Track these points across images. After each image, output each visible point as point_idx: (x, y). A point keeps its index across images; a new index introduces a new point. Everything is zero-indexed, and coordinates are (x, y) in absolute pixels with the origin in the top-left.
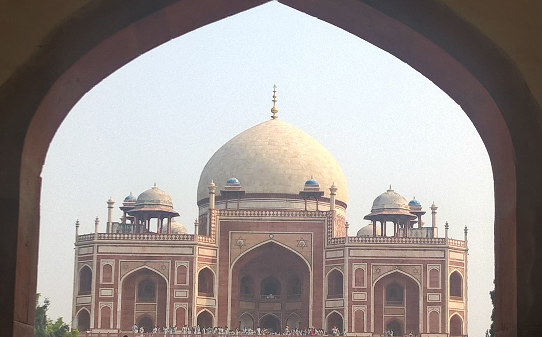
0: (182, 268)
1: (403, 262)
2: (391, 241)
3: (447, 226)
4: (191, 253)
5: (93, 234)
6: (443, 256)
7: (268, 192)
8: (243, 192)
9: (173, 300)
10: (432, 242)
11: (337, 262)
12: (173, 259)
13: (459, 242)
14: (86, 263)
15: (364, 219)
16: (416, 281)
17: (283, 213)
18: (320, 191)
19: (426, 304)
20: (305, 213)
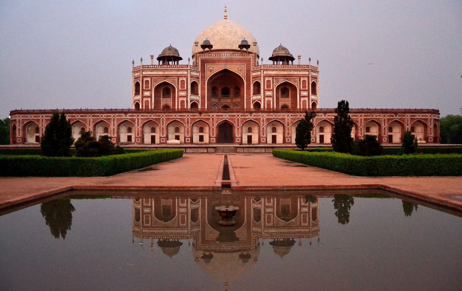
0: (183, 81)
1: (289, 76)
2: (283, 67)
3: (310, 59)
4: (187, 74)
5: (140, 66)
6: (308, 74)
7: (224, 49)
8: (211, 46)
9: (179, 97)
10: (303, 67)
11: (258, 77)
12: (178, 77)
13: (315, 68)
14: (137, 80)
15: (269, 59)
16: (296, 86)
17: (231, 55)
18: (249, 44)
19: (300, 97)
20: (242, 55)
